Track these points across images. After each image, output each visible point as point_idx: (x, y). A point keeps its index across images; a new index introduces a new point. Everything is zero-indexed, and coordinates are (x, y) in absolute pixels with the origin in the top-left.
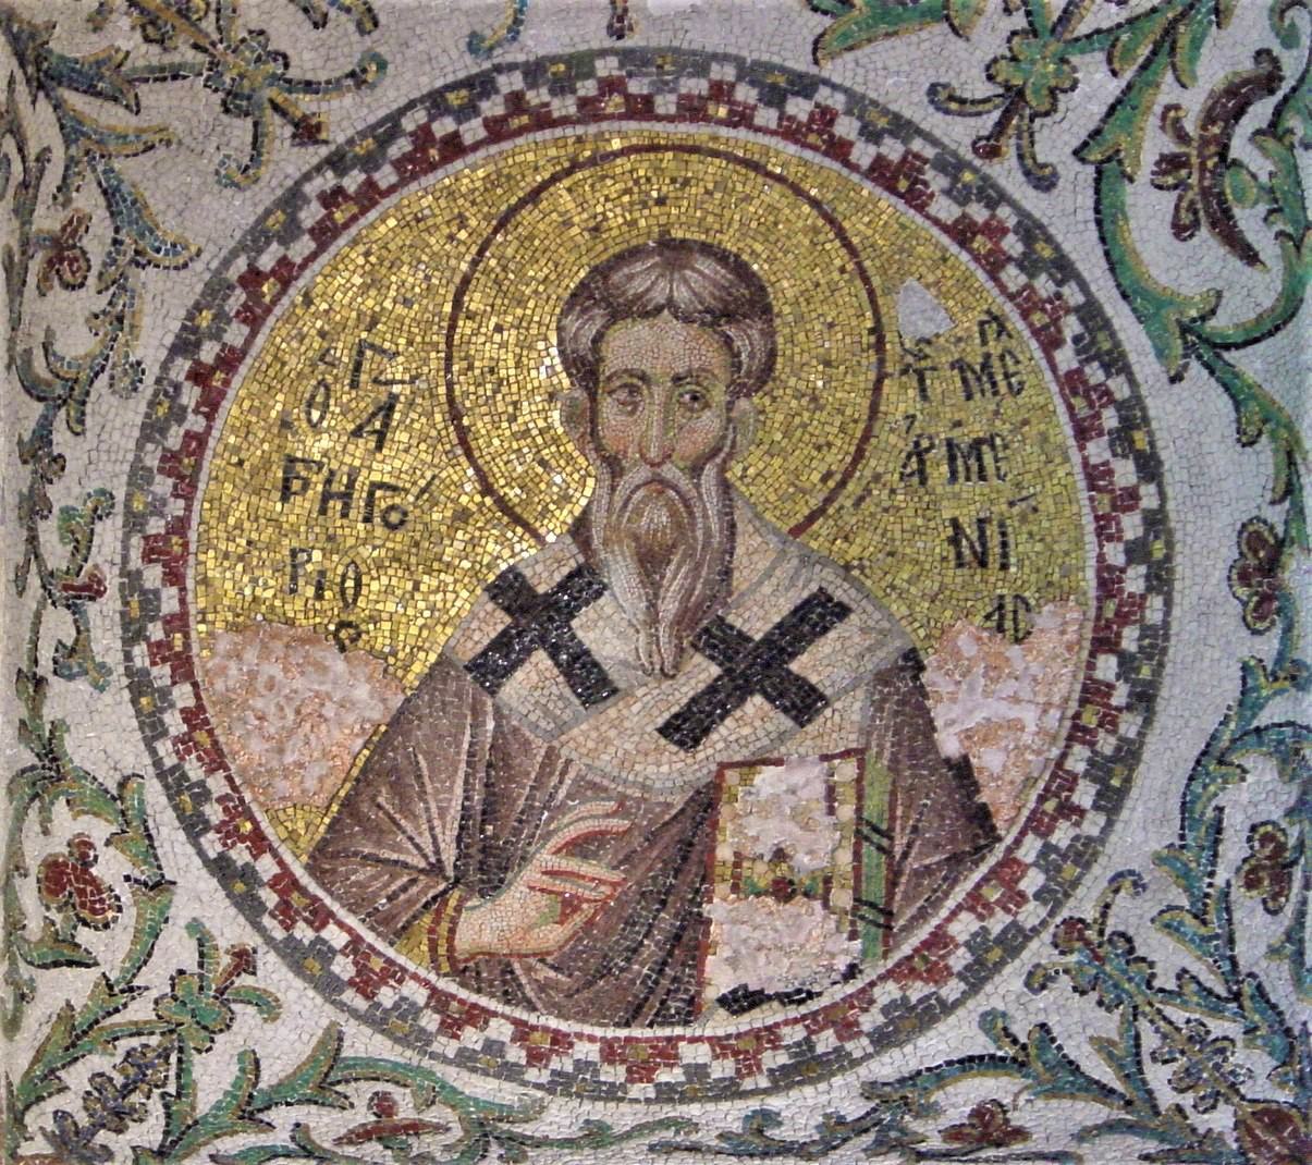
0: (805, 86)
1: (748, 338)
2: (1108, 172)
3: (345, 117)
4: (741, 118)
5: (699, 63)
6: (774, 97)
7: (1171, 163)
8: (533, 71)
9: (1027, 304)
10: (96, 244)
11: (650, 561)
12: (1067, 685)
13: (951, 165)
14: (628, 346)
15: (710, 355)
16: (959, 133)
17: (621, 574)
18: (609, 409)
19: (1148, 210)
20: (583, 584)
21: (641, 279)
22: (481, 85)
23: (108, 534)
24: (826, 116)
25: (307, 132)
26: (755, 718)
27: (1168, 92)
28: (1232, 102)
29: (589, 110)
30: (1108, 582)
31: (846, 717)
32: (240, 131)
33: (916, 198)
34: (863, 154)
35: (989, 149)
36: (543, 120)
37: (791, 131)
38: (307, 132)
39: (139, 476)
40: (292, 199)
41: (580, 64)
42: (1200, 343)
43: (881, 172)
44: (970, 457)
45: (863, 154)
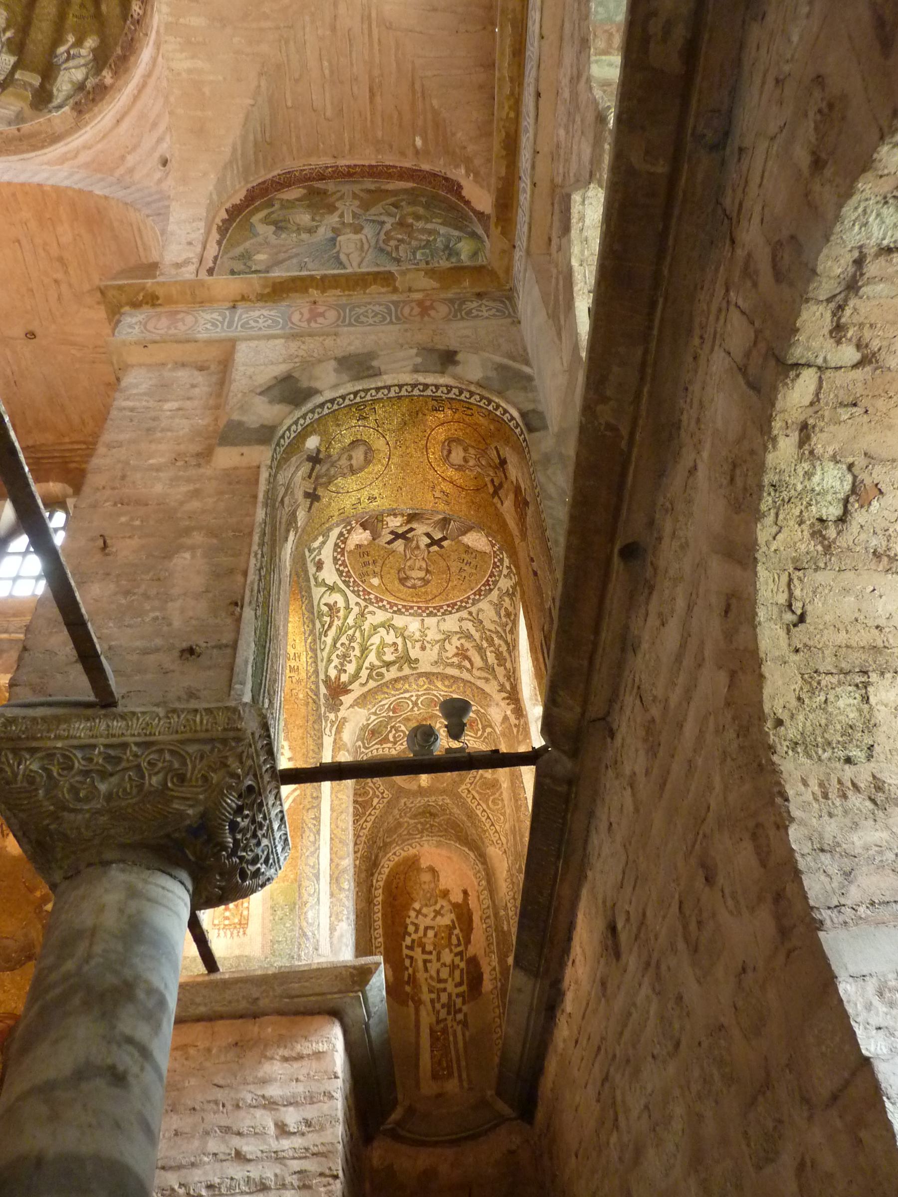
0: (395, 612)
1: (402, 575)
2: (348, 608)
3: (464, 614)
4: (404, 606)
5: (411, 614)
6: (399, 610)
7: (339, 611)
8: (436, 615)
9: (358, 585)
10: (503, 613)
11: (418, 547)
12: (348, 542)
13: (372, 603)
14: (422, 574)
15: (408, 573)
16: (371, 608)
17: (422, 546)
18: (424, 566)
19: (341, 604)
20: (428, 546)
21: (419, 583)
22: (443, 614)
23: (505, 572)
24: (391, 608)
25: (470, 613)
26: (400, 531)
27: (340, 623)
28: (330, 627)
29: (427, 608)
30: (343, 555)
31: (385, 532)
32: (480, 617)
33: (376, 597)
34: (385, 603)
35: (366, 607)
36: (434, 608)
37: (396, 605)
38: (470, 613)
39: (500, 576)
40: (473, 604)
41: (428, 615)
42: (332, 589)
43: (382, 600)
44: (366, 564)
45: (385, 603)
